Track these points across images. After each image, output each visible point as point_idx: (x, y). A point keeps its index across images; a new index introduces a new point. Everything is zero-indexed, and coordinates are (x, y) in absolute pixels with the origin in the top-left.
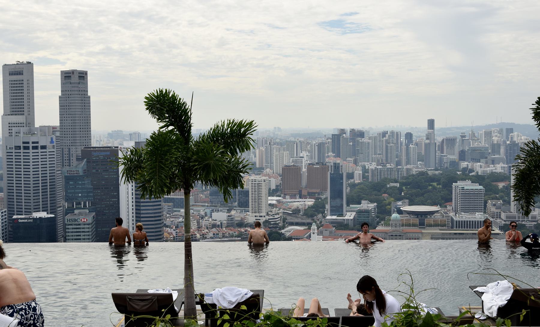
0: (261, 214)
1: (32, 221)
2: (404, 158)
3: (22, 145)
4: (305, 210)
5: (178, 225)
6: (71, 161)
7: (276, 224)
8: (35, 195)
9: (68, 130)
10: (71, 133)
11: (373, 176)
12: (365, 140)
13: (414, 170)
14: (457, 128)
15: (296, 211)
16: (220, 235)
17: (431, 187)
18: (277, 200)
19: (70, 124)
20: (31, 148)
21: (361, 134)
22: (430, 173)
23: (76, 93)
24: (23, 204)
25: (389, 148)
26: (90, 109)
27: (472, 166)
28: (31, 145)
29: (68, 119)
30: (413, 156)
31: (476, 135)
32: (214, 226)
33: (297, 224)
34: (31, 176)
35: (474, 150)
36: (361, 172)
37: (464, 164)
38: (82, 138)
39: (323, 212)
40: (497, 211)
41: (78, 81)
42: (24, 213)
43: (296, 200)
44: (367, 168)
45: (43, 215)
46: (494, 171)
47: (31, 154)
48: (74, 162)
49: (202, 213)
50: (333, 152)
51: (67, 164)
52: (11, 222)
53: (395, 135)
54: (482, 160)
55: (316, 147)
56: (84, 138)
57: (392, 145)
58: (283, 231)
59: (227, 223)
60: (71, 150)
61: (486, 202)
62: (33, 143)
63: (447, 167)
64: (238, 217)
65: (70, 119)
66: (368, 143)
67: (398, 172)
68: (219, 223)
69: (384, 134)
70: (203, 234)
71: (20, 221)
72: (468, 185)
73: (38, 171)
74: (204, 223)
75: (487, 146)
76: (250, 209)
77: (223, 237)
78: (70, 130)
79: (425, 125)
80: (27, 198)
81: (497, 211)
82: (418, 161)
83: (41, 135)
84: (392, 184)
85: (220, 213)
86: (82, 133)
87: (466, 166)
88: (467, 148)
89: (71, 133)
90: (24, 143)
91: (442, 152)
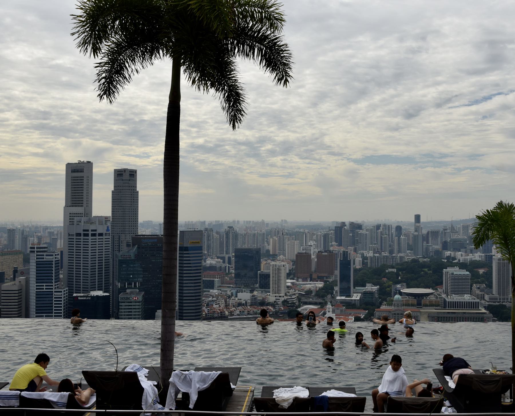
0: (281, 295)
1: (90, 298)
2: (396, 247)
3: (82, 233)
4: (317, 291)
5: (208, 303)
6: (121, 247)
7: (293, 303)
8: (92, 276)
9: (119, 220)
10: (121, 222)
11: (371, 262)
12: (363, 232)
13: (406, 258)
14: (436, 222)
15: (309, 292)
16: (246, 312)
17: (422, 273)
18: (291, 283)
19: (121, 215)
20: (90, 235)
21: (359, 227)
22: (421, 260)
23: (127, 188)
24: (82, 284)
25: (383, 239)
26: (138, 202)
27: (455, 254)
28: (90, 233)
29: (119, 210)
30: (404, 245)
31: (455, 228)
32: (240, 304)
33: (310, 303)
34: (90, 260)
35: (455, 241)
36: (361, 259)
37: (448, 253)
38: (131, 227)
39: (332, 293)
40: (480, 293)
41: (129, 178)
42: (81, 291)
43: (308, 283)
44: (365, 255)
45: (100, 293)
46: (473, 259)
47: (90, 241)
48: (124, 248)
49: (229, 293)
50: (336, 242)
51: (117, 249)
52: (72, 299)
53: (388, 227)
54: (461, 249)
55: (322, 238)
56: (133, 227)
57: (386, 236)
58: (299, 309)
59: (251, 302)
60: (121, 237)
61: (471, 286)
62: (92, 231)
63: (432, 256)
64: (259, 297)
65: (121, 210)
66: (366, 234)
67: (393, 259)
68: (244, 302)
69: (378, 227)
70: (231, 312)
71: (79, 298)
72: (456, 271)
73: (96, 255)
74: (231, 302)
75: (466, 237)
76: (271, 290)
77: (248, 314)
78: (121, 220)
79: (413, 220)
80: (84, 278)
81: (480, 293)
82: (408, 250)
83: (99, 224)
84: (390, 270)
85: (244, 294)
86: (131, 222)
87: (449, 255)
88: (449, 240)
89: (121, 222)
90: (84, 230)
91: (428, 243)
